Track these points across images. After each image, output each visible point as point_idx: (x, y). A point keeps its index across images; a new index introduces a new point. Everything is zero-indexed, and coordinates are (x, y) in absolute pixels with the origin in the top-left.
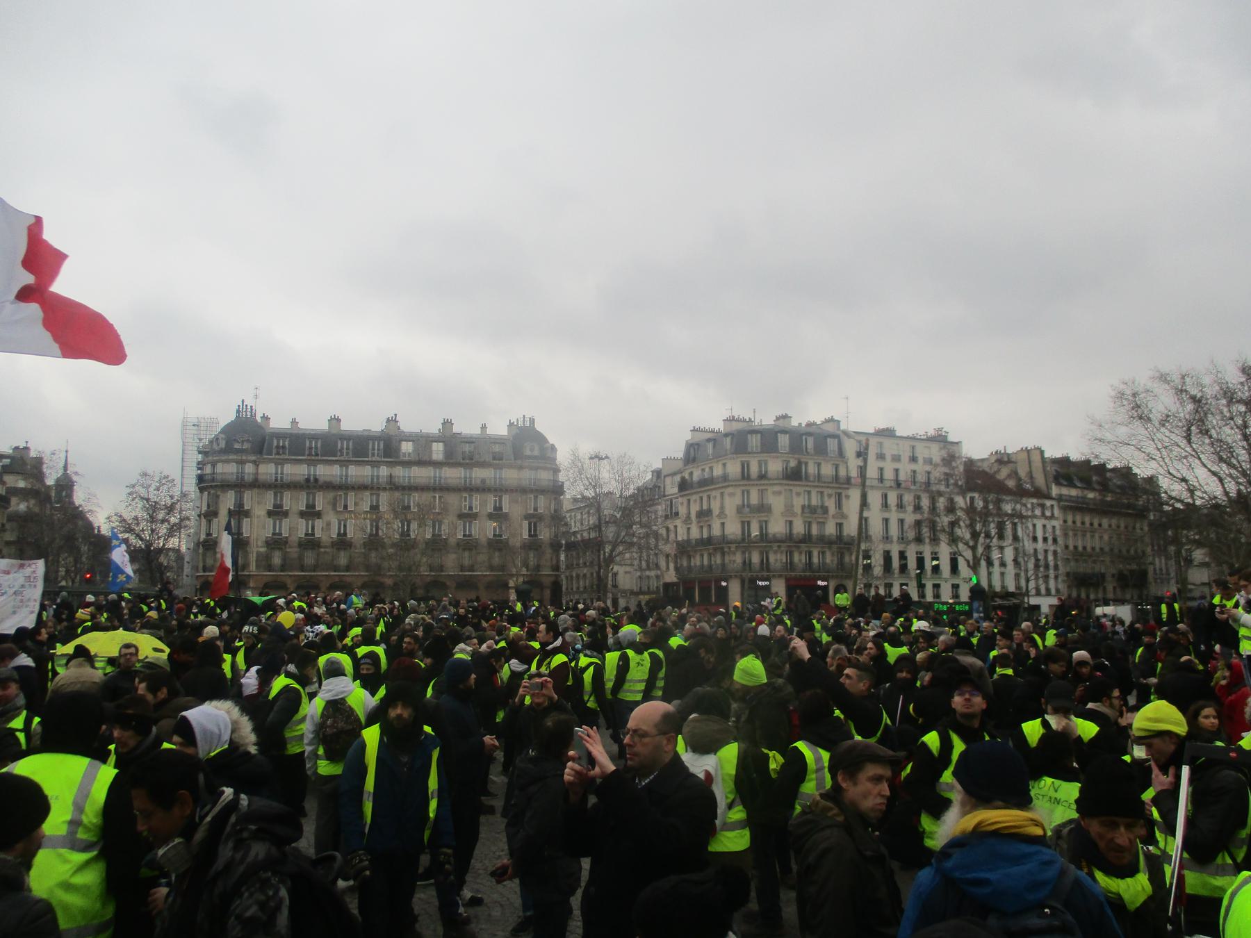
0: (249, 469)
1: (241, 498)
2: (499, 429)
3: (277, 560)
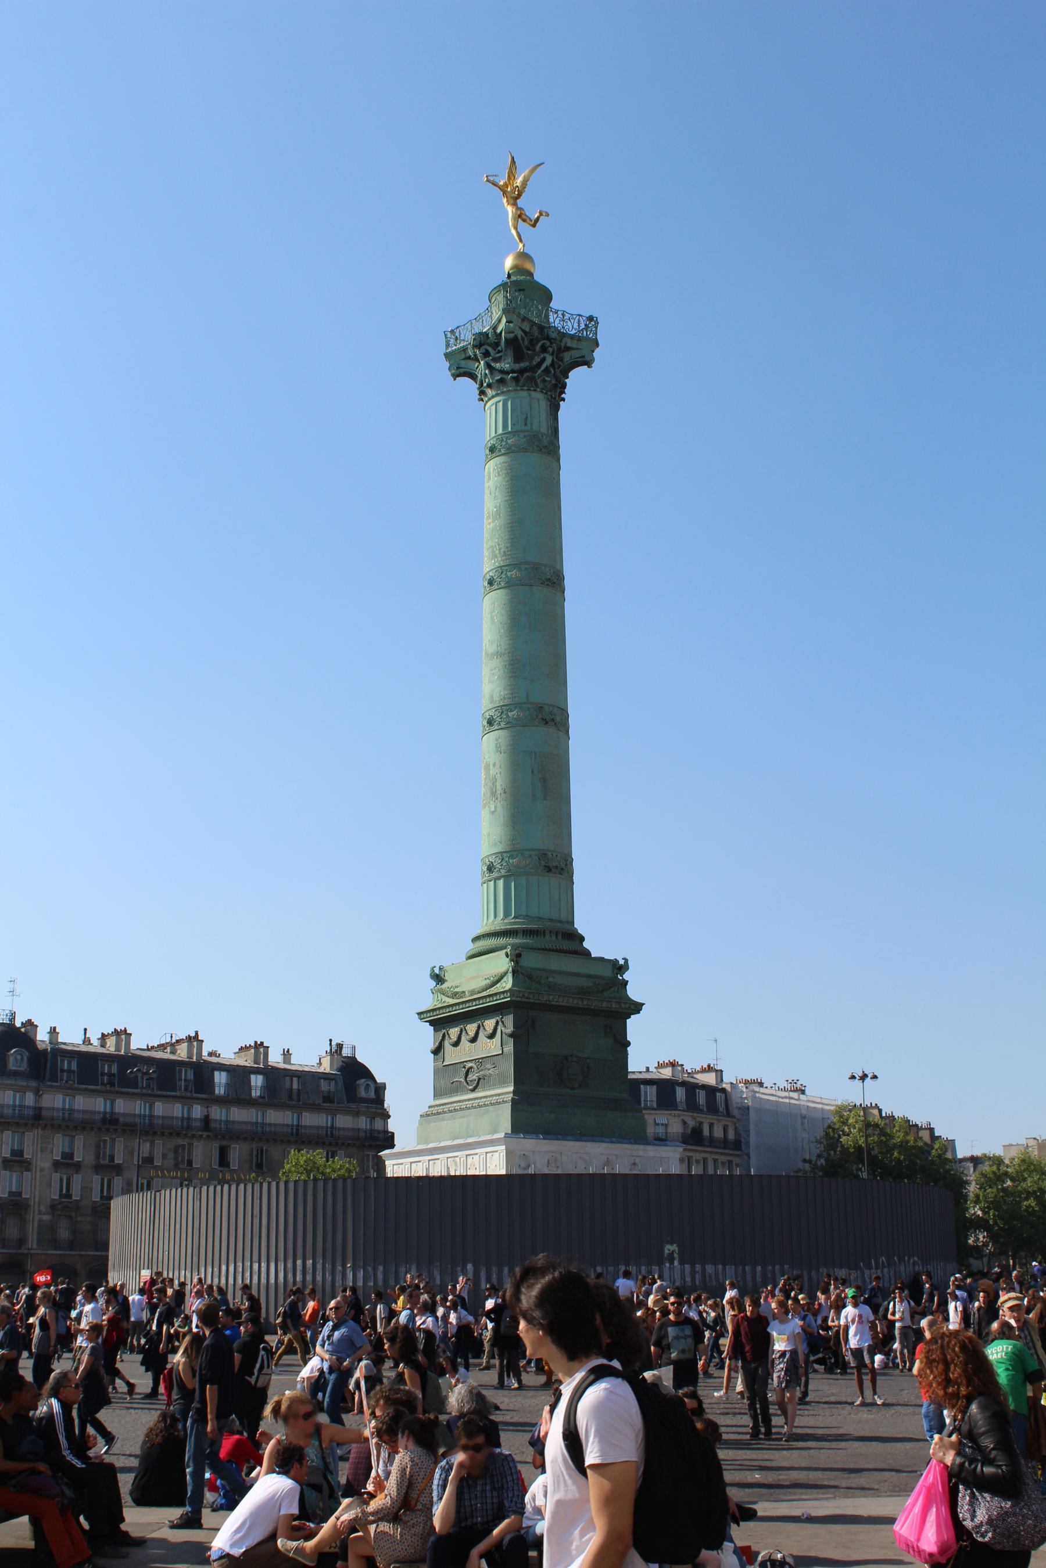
0: (30, 1099)
1: (21, 1142)
2: (310, 1056)
3: (64, 1233)
